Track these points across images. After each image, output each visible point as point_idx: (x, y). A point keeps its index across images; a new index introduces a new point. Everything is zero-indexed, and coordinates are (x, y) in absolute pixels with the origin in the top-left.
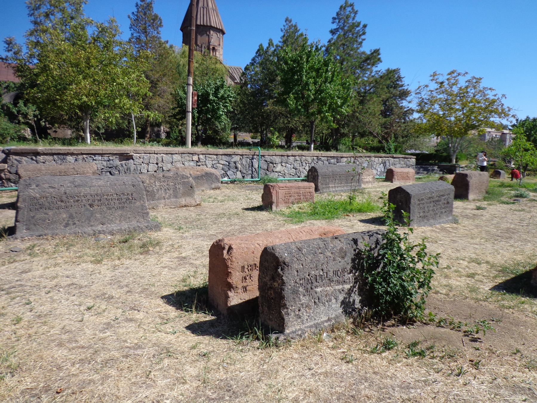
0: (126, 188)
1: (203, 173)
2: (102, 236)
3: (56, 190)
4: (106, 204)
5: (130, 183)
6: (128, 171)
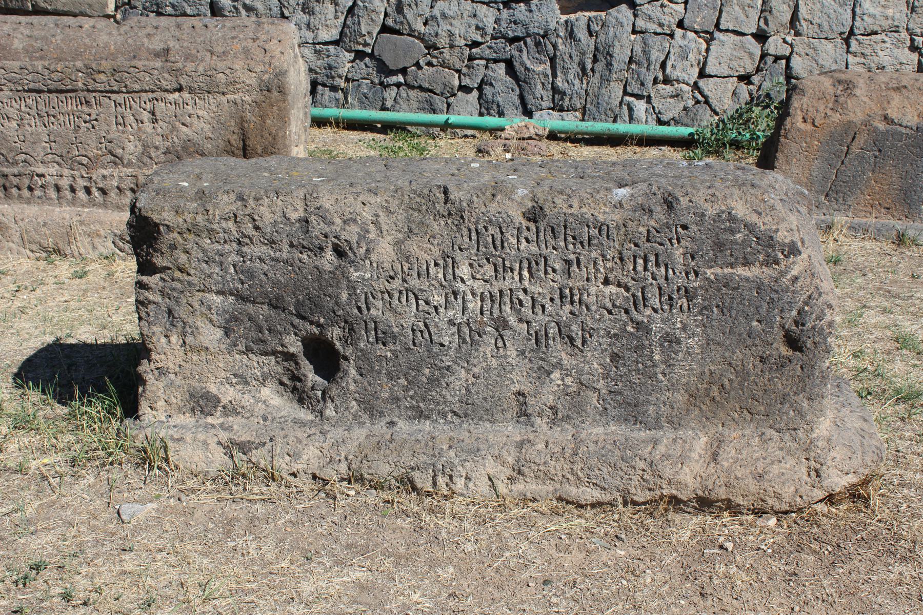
6: (600, 66)
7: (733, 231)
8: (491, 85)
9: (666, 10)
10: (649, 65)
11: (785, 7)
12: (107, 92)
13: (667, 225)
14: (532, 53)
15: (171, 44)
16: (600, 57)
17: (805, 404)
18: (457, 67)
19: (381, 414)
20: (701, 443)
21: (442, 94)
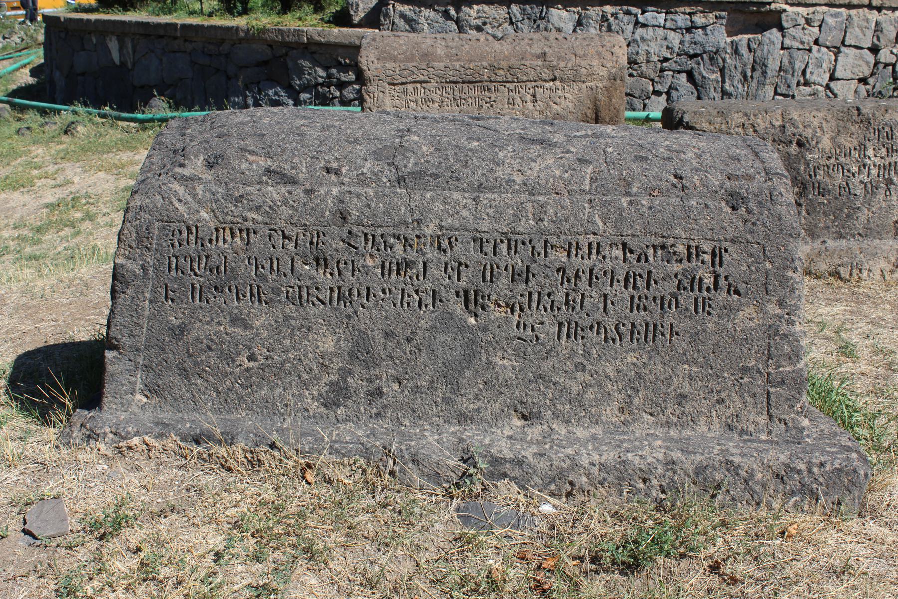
0: (687, 212)
3: (299, 192)
4: (559, 297)
5: (715, 181)
6: (757, 74)
8: (677, 90)
9: (806, 32)
10: (793, 72)
12: (504, 82)
14: (707, 65)
15: (547, 50)
16: (757, 67)
18: (652, 77)
19: (819, 236)
21: (640, 97)
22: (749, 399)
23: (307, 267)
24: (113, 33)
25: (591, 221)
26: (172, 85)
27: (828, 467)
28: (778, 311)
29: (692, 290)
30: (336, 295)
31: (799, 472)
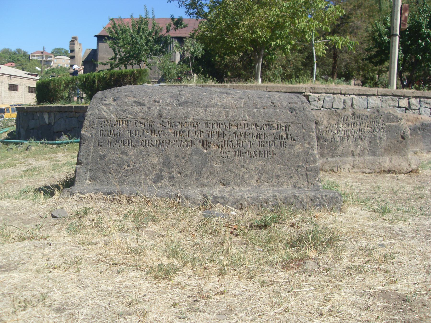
0: (276, 114)
1: (418, 124)
2: (219, 208)
3: (146, 108)
4: (235, 142)
5: (285, 104)
7: (390, 116)
11: (350, 102)
13: (378, 115)
17: (406, 150)
19: (325, 157)
20: (388, 159)
22: (300, 176)
23: (148, 134)
24: (46, 112)
25: (244, 117)
26: (70, 130)
27: (328, 197)
28: (308, 146)
29: (279, 139)
30: (158, 143)
31: (319, 198)
